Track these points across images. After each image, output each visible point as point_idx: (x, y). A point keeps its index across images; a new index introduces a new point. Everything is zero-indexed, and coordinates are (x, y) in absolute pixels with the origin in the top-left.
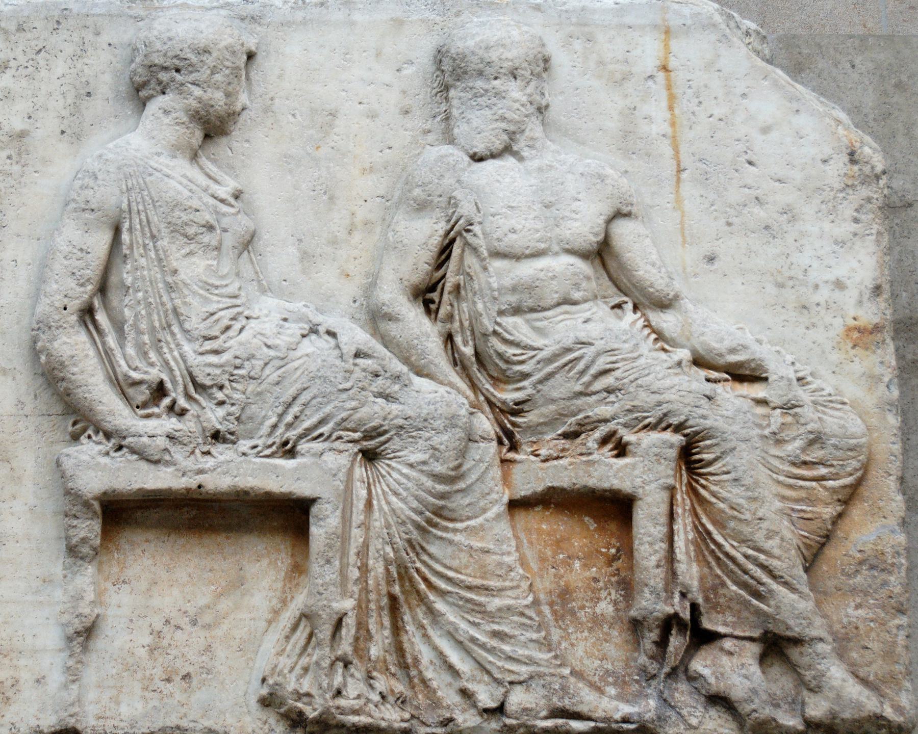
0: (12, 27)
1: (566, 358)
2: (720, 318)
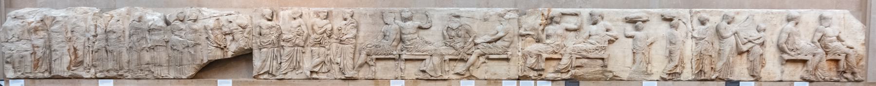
1: (835, 47)
2: (849, 43)
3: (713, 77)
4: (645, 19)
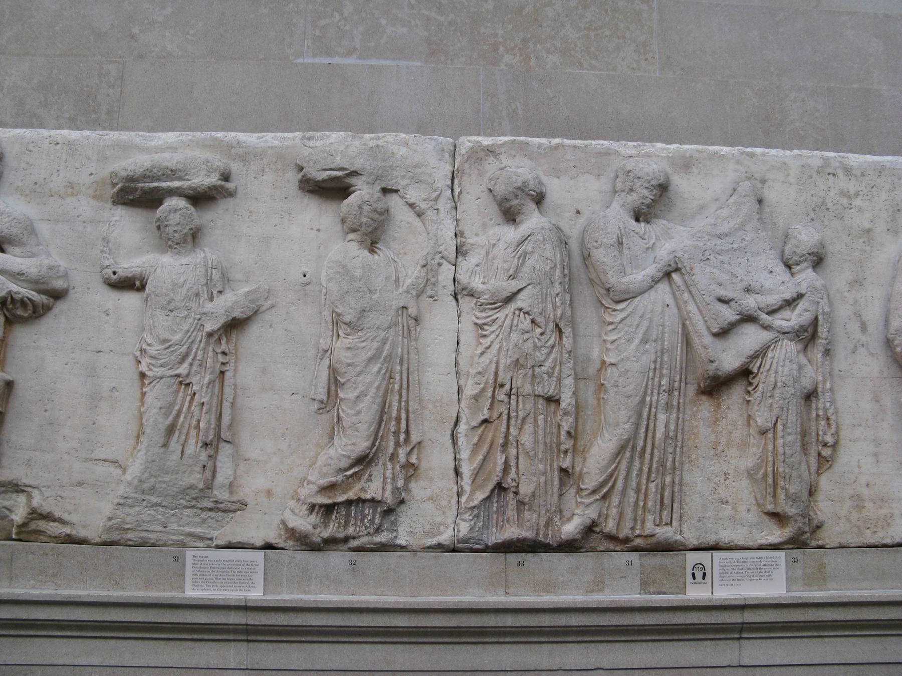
0: (859, 174)
3: (570, 529)
4: (201, 180)
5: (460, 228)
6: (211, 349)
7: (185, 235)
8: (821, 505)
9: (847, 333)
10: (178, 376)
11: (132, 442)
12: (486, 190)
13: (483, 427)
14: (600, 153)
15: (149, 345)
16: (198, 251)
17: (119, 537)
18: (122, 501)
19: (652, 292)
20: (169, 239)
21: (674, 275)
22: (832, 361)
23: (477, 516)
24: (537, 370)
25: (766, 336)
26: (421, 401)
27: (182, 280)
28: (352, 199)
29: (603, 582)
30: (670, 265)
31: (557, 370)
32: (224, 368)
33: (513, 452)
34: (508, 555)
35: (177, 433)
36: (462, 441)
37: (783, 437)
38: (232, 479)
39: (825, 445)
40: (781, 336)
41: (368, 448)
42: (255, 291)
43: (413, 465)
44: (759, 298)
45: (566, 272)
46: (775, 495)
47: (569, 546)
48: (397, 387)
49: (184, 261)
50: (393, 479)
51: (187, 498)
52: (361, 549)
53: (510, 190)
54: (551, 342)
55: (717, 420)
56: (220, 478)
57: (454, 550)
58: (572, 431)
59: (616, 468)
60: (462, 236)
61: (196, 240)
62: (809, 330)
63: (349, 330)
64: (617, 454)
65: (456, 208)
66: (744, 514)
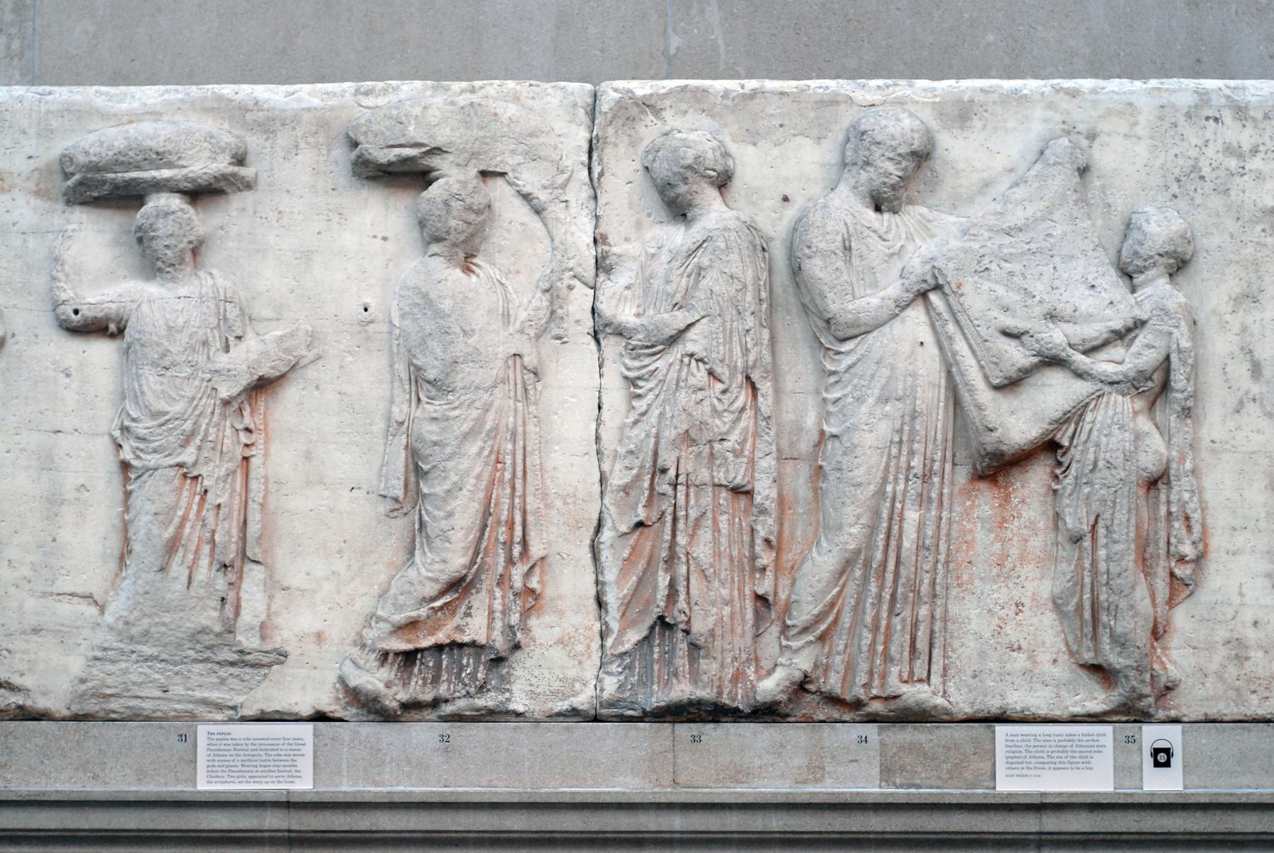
0: (1260, 116)
3: (770, 686)
4: (203, 165)
5: (601, 230)
6: (228, 423)
7: (182, 251)
8: (1174, 654)
9: (1227, 381)
10: (180, 465)
11: (113, 565)
12: (640, 167)
13: (637, 533)
14: (822, 102)
15: (134, 420)
16: (202, 274)
17: (97, 708)
18: (99, 654)
19: (896, 324)
20: (158, 259)
21: (934, 298)
22: (1197, 424)
23: (630, 667)
24: (717, 446)
25: (1082, 388)
26: (545, 495)
27: (180, 321)
28: (434, 190)
29: (823, 768)
30: (925, 281)
31: (748, 445)
32: (247, 453)
33: (683, 569)
34: (677, 725)
35: (181, 550)
36: (606, 555)
37: (1106, 546)
38: (263, 617)
39: (1182, 559)
40: (1107, 389)
41: (464, 567)
42: (292, 335)
43: (533, 591)
44: (1069, 328)
45: (764, 295)
46: (1095, 637)
47: (767, 712)
48: (508, 476)
49: (183, 291)
50: (503, 612)
51: (198, 647)
52: (458, 718)
53: (676, 169)
54: (739, 404)
55: (1005, 520)
56: (246, 617)
57: (596, 719)
58: (772, 538)
59: (840, 592)
60: (604, 243)
61: (199, 259)
62: (1155, 376)
63: (434, 392)
64: (841, 573)
65: (596, 198)
66: (1047, 667)
